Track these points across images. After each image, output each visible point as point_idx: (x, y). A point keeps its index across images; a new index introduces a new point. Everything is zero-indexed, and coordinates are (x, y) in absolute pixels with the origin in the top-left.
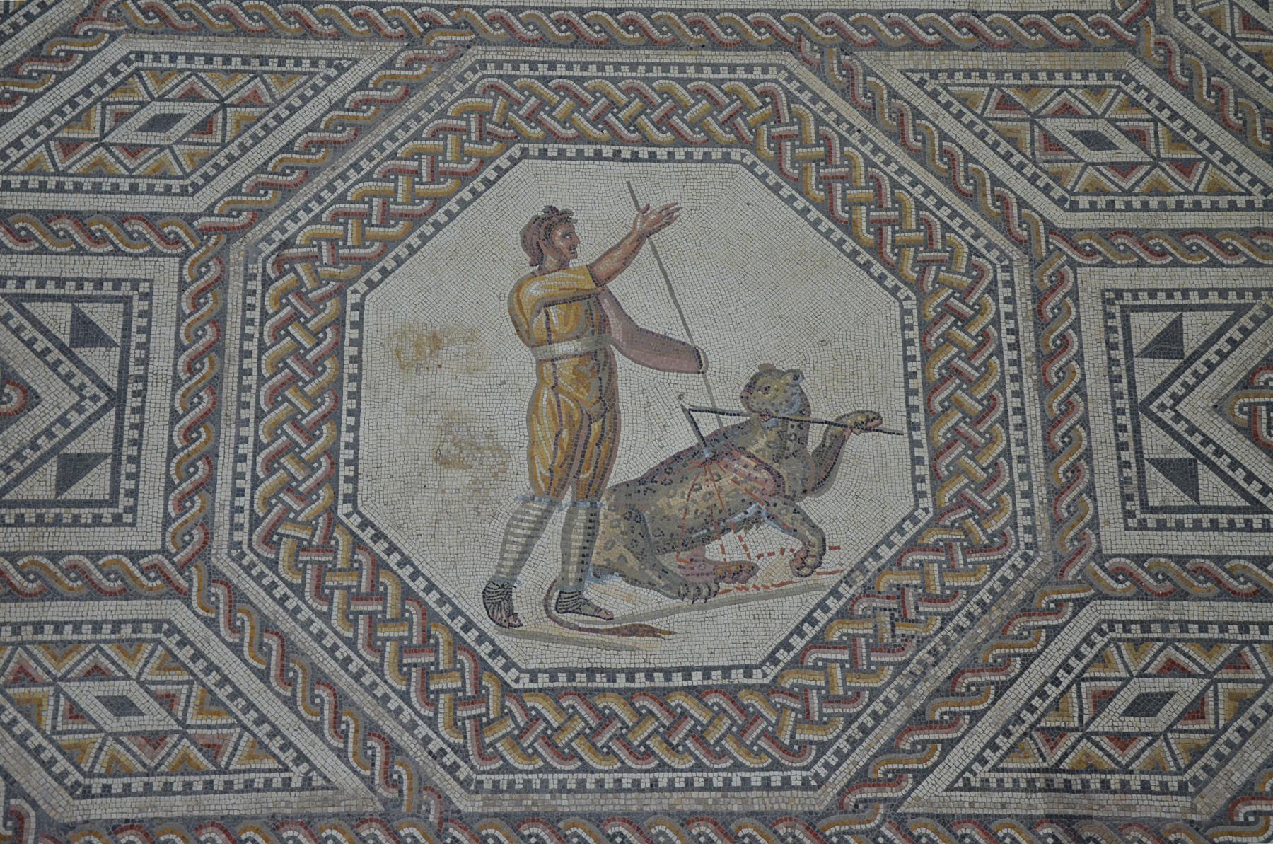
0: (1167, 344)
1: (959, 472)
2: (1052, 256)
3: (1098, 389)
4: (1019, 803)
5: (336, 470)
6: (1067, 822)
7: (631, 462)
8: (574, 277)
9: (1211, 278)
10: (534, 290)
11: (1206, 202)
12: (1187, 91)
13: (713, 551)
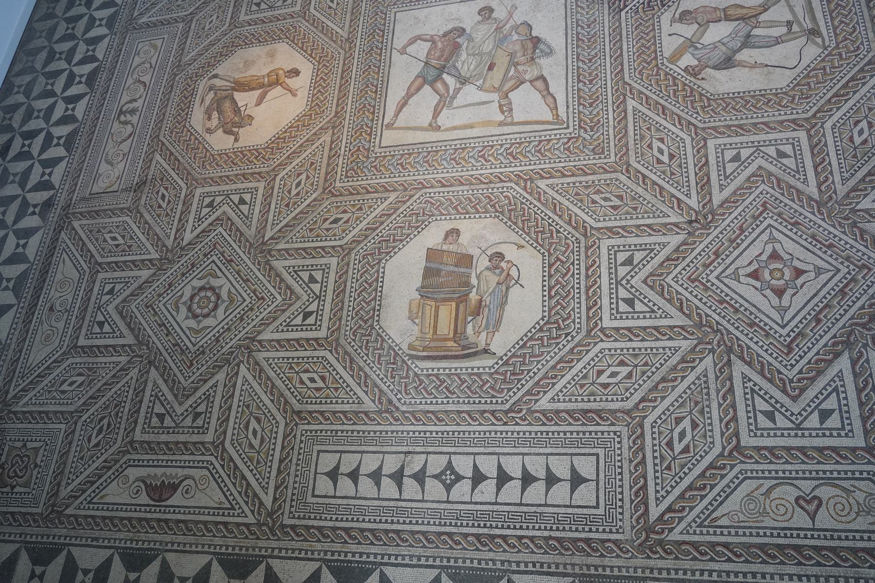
0: (242, 201)
1: (221, 159)
2: (270, 178)
3: (234, 187)
4: (151, 173)
5: (248, 44)
6: (145, 182)
7: (237, 96)
8: (282, 78)
9: (257, 210)
10: (281, 72)
11: (277, 210)
12: (309, 205)
13: (215, 112)
